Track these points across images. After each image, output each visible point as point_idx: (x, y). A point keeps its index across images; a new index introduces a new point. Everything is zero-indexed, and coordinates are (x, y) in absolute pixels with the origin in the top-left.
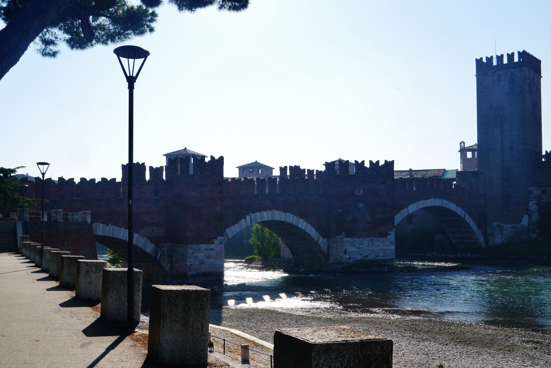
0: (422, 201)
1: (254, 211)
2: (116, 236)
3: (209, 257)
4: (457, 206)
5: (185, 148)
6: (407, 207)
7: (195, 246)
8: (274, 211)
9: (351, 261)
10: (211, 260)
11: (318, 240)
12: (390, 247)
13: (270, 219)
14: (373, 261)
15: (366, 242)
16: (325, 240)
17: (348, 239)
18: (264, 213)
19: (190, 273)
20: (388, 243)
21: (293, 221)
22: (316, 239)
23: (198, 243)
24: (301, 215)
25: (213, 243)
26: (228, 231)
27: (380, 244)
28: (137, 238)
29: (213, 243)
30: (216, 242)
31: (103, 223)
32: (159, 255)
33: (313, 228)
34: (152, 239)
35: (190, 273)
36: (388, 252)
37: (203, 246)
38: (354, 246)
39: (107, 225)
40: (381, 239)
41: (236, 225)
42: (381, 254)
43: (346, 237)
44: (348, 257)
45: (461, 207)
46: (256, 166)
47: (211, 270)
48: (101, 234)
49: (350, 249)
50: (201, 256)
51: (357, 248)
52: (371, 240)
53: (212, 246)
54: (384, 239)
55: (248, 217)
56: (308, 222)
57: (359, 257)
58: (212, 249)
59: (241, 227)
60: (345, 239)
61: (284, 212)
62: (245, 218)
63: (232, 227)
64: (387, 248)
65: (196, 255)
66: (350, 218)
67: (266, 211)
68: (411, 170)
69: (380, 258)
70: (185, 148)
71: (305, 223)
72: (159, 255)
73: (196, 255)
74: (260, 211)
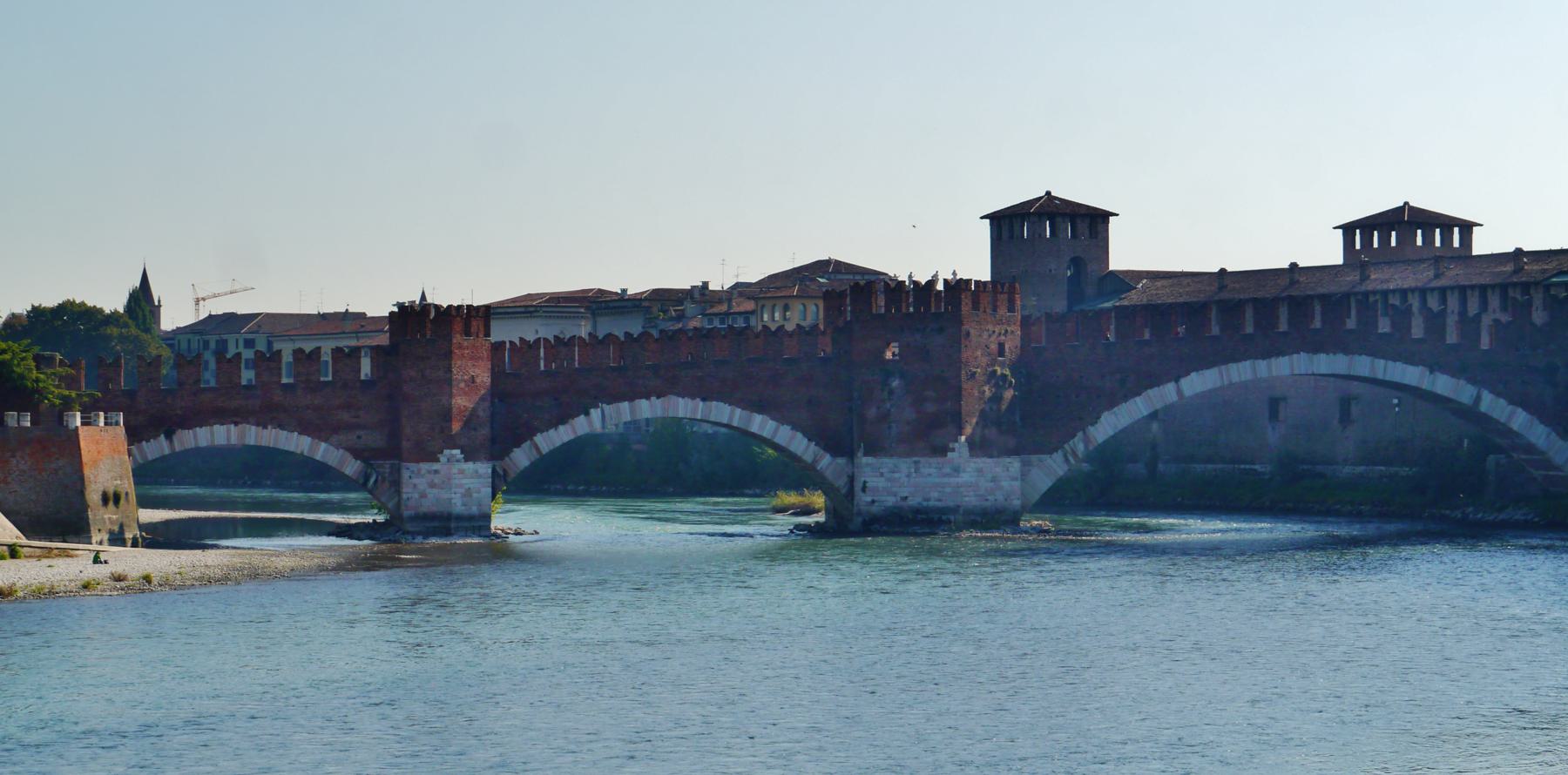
0: (1248, 363)
1: (614, 399)
2: (281, 446)
3: (432, 485)
4: (1431, 372)
5: (1048, 193)
6: (1177, 381)
7: (413, 466)
8: (673, 398)
9: (875, 509)
10: (435, 491)
11: (815, 461)
12: (953, 480)
13: (659, 413)
14: (917, 511)
15: (905, 465)
16: (841, 461)
17: (870, 460)
18: (644, 403)
19: (406, 513)
20: (947, 470)
21: (731, 418)
22: (808, 458)
23: (417, 462)
24: (761, 407)
25: (438, 460)
26: (538, 438)
27: (932, 470)
28: (326, 450)
29: (438, 460)
30: (443, 459)
31: (258, 425)
32: (372, 480)
33: (799, 435)
34: (357, 453)
35: (406, 513)
36: (948, 490)
37: (424, 466)
38: (882, 475)
39: (265, 427)
40: (934, 460)
41: (561, 428)
42: (935, 495)
43: (866, 454)
44: (869, 499)
45: (1456, 372)
46: (1405, 219)
47: (435, 509)
48: (252, 443)
49: (874, 481)
50: (421, 483)
51: (888, 480)
52: (916, 463)
53: (436, 466)
54: (940, 460)
55: (595, 414)
56: (782, 420)
57: (890, 501)
58: (436, 472)
59: (574, 431)
60: (865, 460)
61: (704, 400)
62: (587, 414)
63: (552, 432)
64: (946, 480)
65: (415, 481)
66: (872, 412)
67: (648, 397)
68: (1519, 252)
69: (932, 503)
70: (1048, 193)
71: (771, 424)
72: (372, 480)
73: (415, 481)
74: (631, 399)
